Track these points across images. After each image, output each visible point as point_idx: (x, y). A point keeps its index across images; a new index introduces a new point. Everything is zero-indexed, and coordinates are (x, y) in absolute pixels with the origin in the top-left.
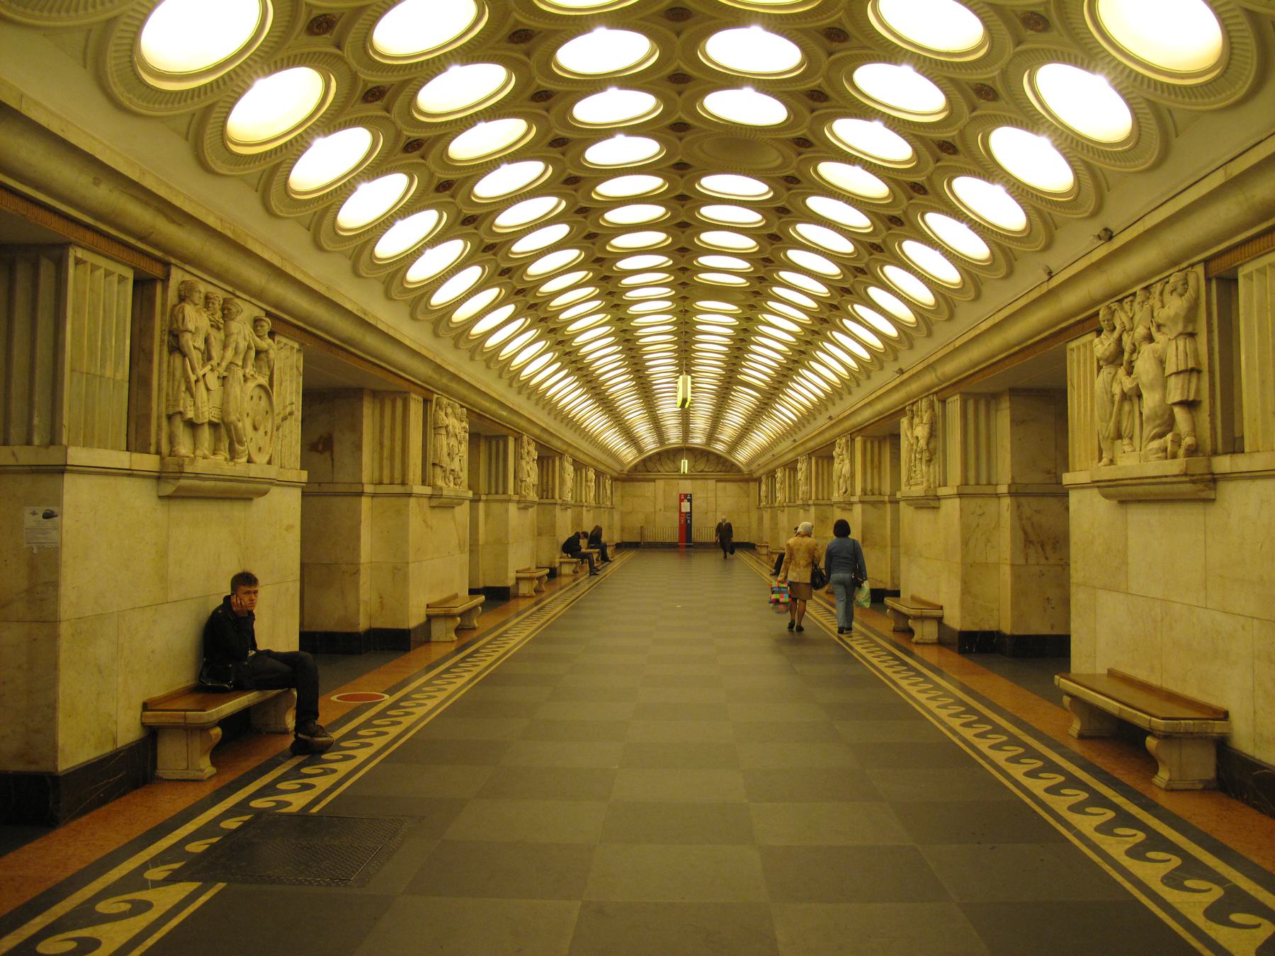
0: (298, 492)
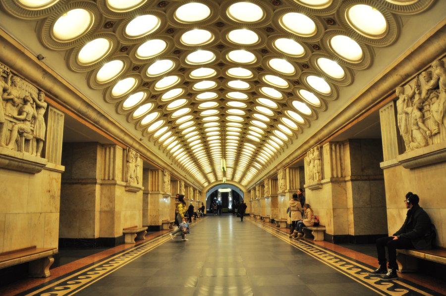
0: (60, 175)
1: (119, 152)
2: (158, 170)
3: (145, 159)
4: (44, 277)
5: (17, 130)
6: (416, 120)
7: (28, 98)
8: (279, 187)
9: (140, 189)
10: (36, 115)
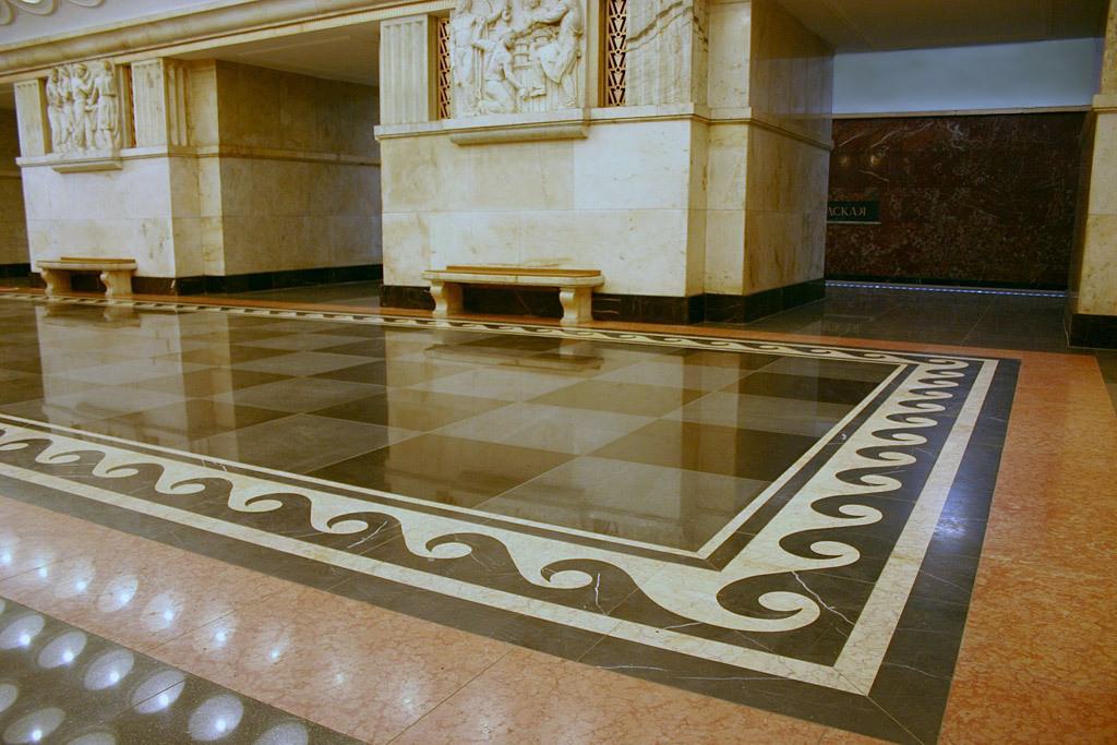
6: (502, 65)
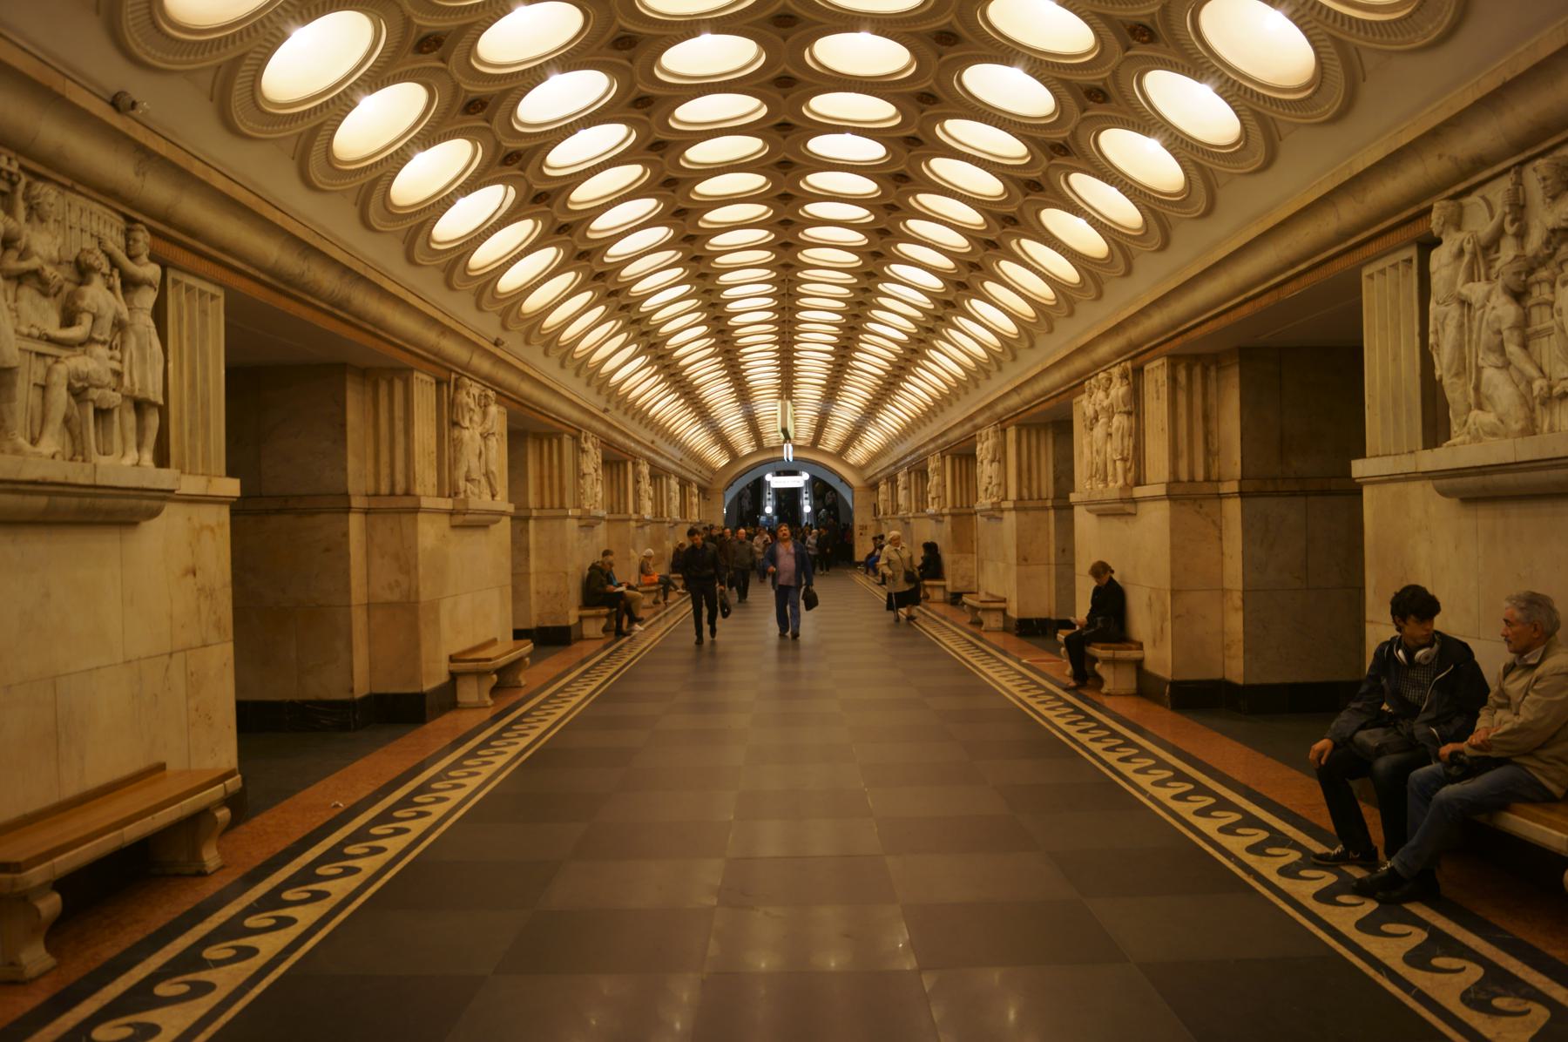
1: (424, 393)
2: (558, 435)
3: (516, 406)
4: (202, 874)
5: (65, 382)
6: (1499, 332)
7: (91, 259)
8: (981, 488)
9: (503, 513)
10: (126, 316)
